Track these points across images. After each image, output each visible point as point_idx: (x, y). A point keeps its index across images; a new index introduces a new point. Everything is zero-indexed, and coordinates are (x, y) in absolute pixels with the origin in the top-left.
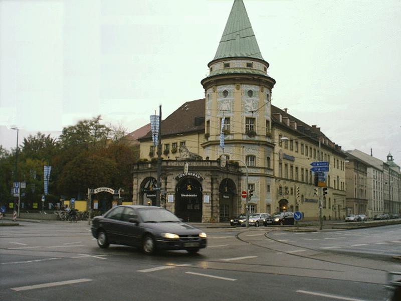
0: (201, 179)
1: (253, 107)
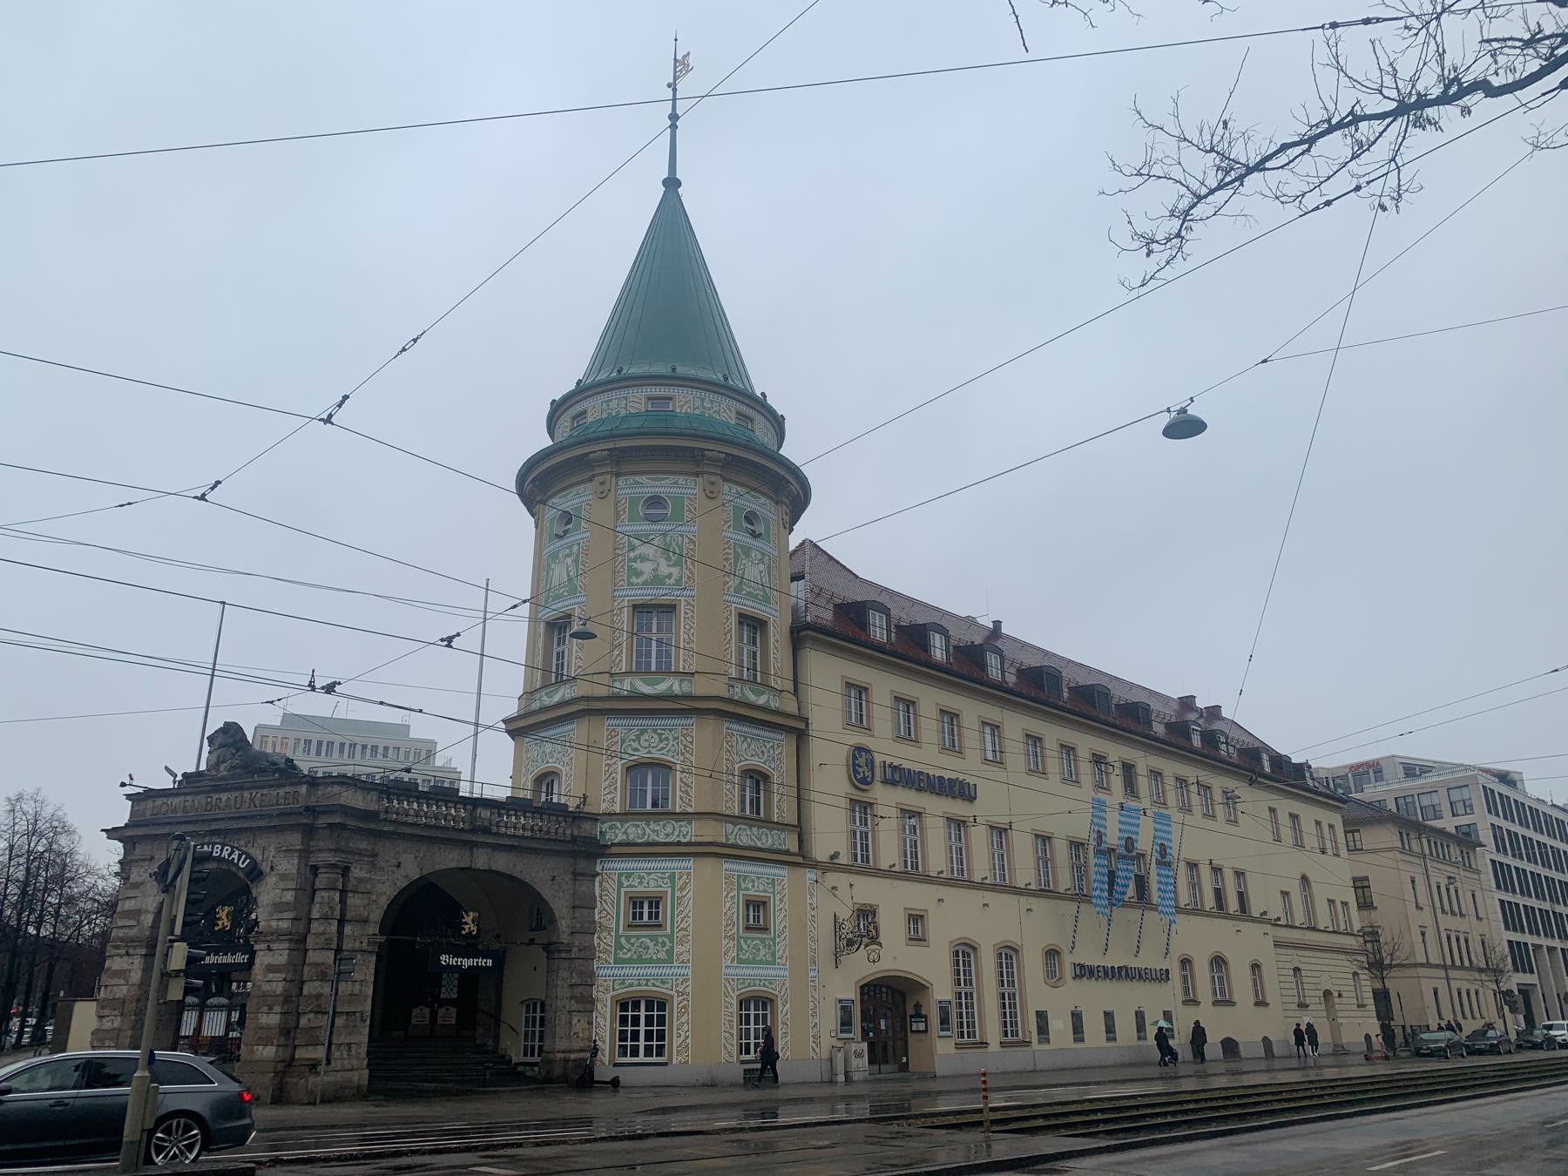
0: (255, 873)
1: (663, 562)
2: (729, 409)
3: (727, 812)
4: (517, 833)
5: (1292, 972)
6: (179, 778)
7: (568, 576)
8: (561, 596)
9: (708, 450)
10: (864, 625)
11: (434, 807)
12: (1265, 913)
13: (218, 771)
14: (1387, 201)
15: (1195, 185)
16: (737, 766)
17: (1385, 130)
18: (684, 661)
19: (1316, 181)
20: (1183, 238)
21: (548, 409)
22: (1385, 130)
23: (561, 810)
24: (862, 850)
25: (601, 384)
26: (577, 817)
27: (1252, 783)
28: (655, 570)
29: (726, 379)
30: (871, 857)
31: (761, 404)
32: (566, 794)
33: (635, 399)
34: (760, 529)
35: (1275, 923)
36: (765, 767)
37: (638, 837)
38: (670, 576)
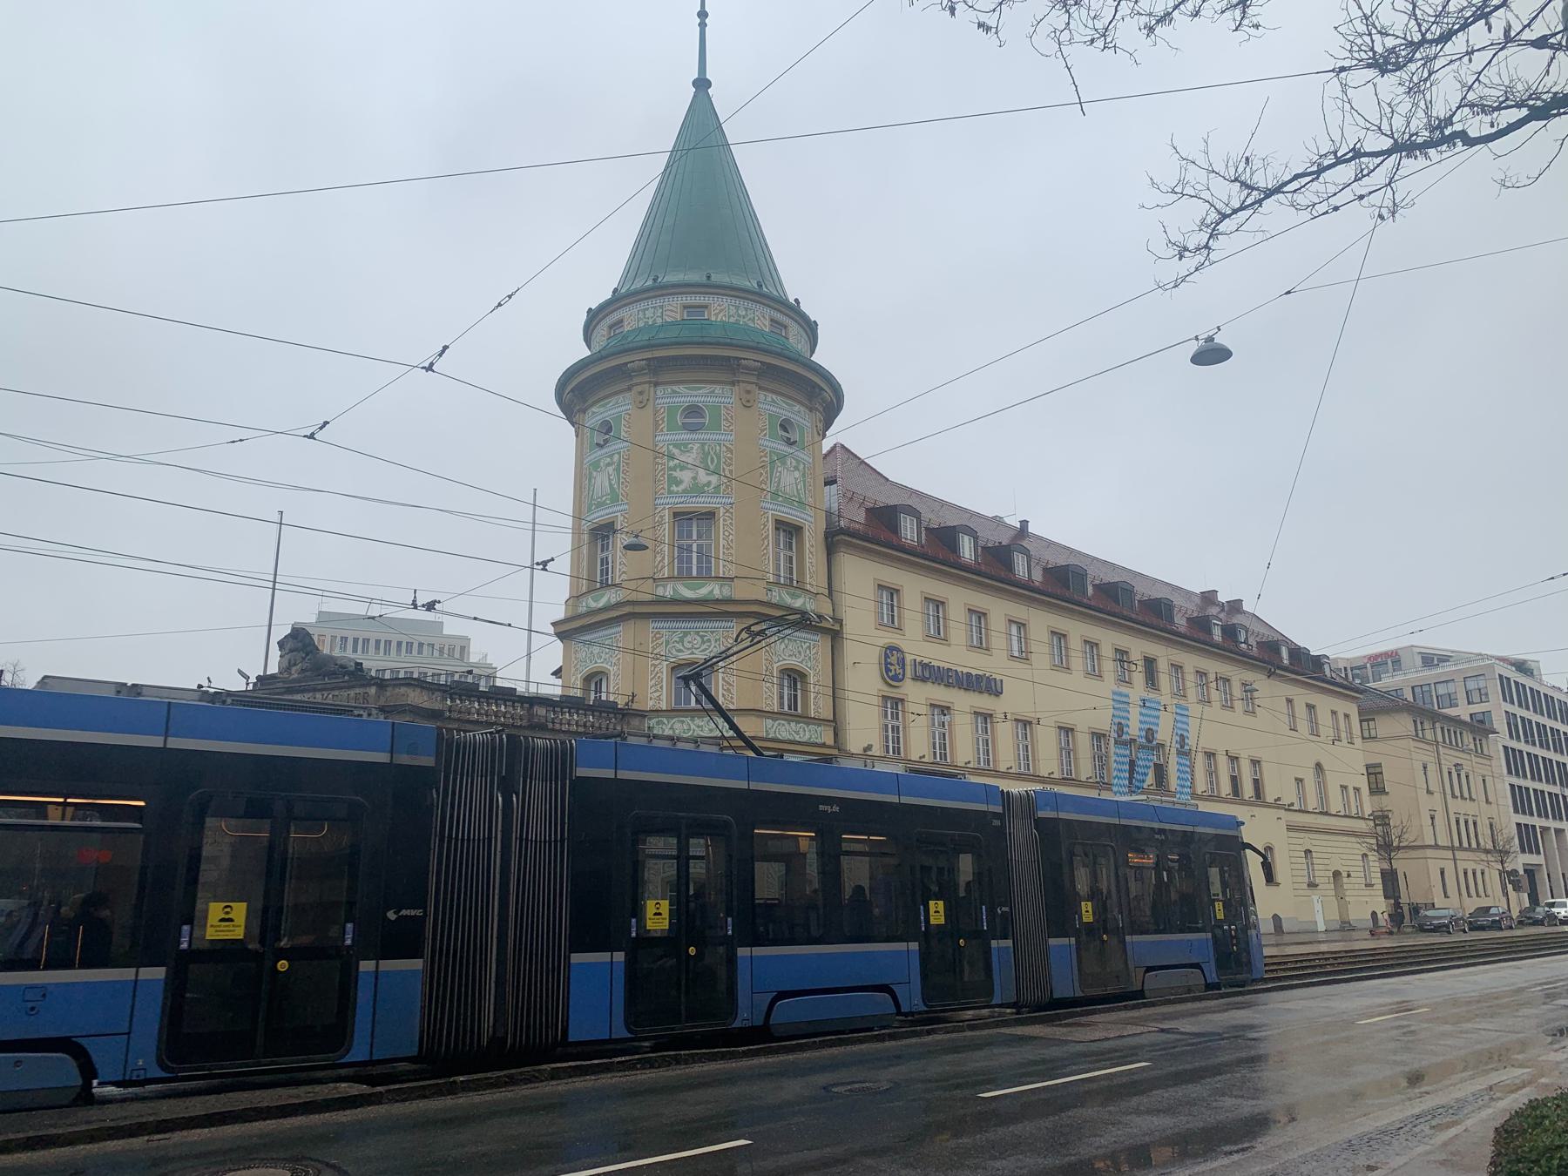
1: (702, 472)
2: (763, 317)
3: (767, 709)
4: (571, 729)
5: (1303, 854)
6: (253, 680)
7: (610, 485)
8: (604, 503)
9: (744, 359)
10: (895, 528)
11: (503, 707)
12: (1279, 799)
13: (290, 674)
14: (1385, 212)
15: (1220, 206)
16: (775, 666)
17: (1381, 163)
18: (724, 566)
19: (1325, 195)
20: (1210, 249)
21: (583, 317)
22: (1381, 163)
23: (611, 708)
24: (893, 743)
25: (636, 293)
26: (625, 714)
27: (1270, 675)
28: (694, 478)
29: (760, 286)
30: (902, 749)
31: (794, 311)
32: (615, 691)
33: (670, 308)
34: (795, 436)
35: (1289, 808)
36: (803, 667)
37: (684, 732)
38: (709, 483)
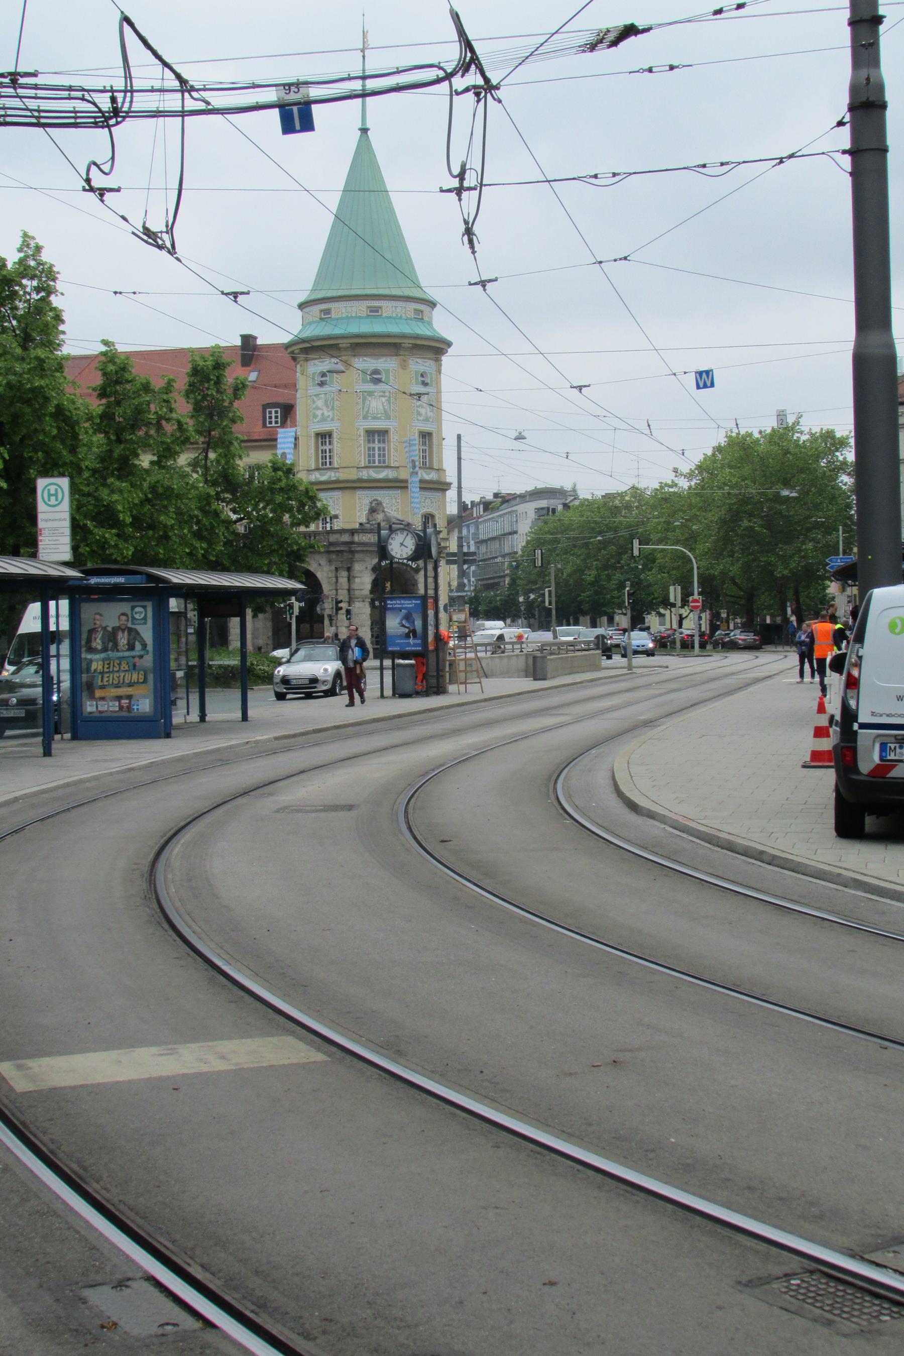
7: (384, 408)
8: (380, 418)
